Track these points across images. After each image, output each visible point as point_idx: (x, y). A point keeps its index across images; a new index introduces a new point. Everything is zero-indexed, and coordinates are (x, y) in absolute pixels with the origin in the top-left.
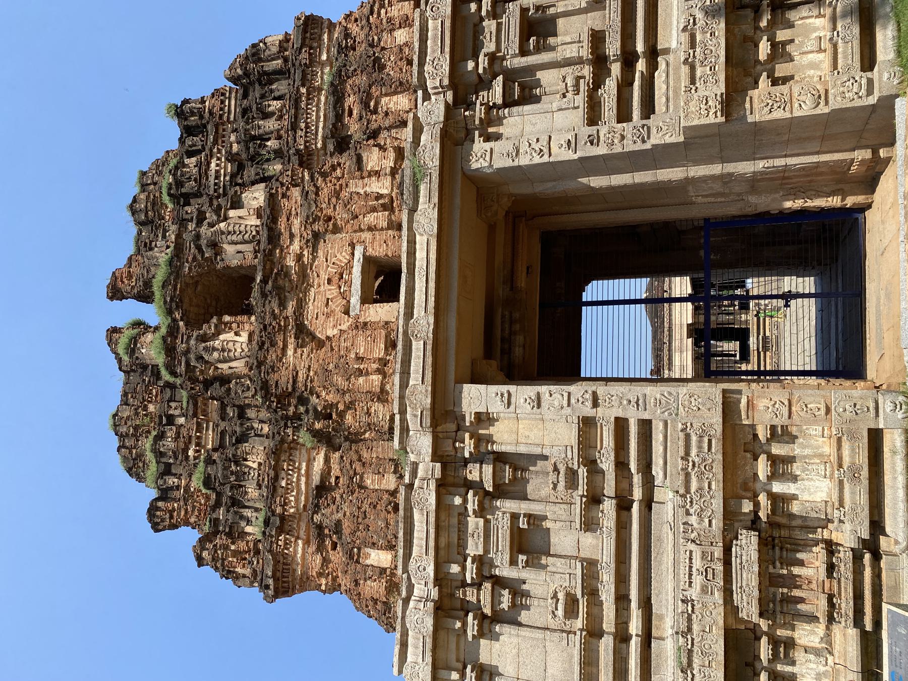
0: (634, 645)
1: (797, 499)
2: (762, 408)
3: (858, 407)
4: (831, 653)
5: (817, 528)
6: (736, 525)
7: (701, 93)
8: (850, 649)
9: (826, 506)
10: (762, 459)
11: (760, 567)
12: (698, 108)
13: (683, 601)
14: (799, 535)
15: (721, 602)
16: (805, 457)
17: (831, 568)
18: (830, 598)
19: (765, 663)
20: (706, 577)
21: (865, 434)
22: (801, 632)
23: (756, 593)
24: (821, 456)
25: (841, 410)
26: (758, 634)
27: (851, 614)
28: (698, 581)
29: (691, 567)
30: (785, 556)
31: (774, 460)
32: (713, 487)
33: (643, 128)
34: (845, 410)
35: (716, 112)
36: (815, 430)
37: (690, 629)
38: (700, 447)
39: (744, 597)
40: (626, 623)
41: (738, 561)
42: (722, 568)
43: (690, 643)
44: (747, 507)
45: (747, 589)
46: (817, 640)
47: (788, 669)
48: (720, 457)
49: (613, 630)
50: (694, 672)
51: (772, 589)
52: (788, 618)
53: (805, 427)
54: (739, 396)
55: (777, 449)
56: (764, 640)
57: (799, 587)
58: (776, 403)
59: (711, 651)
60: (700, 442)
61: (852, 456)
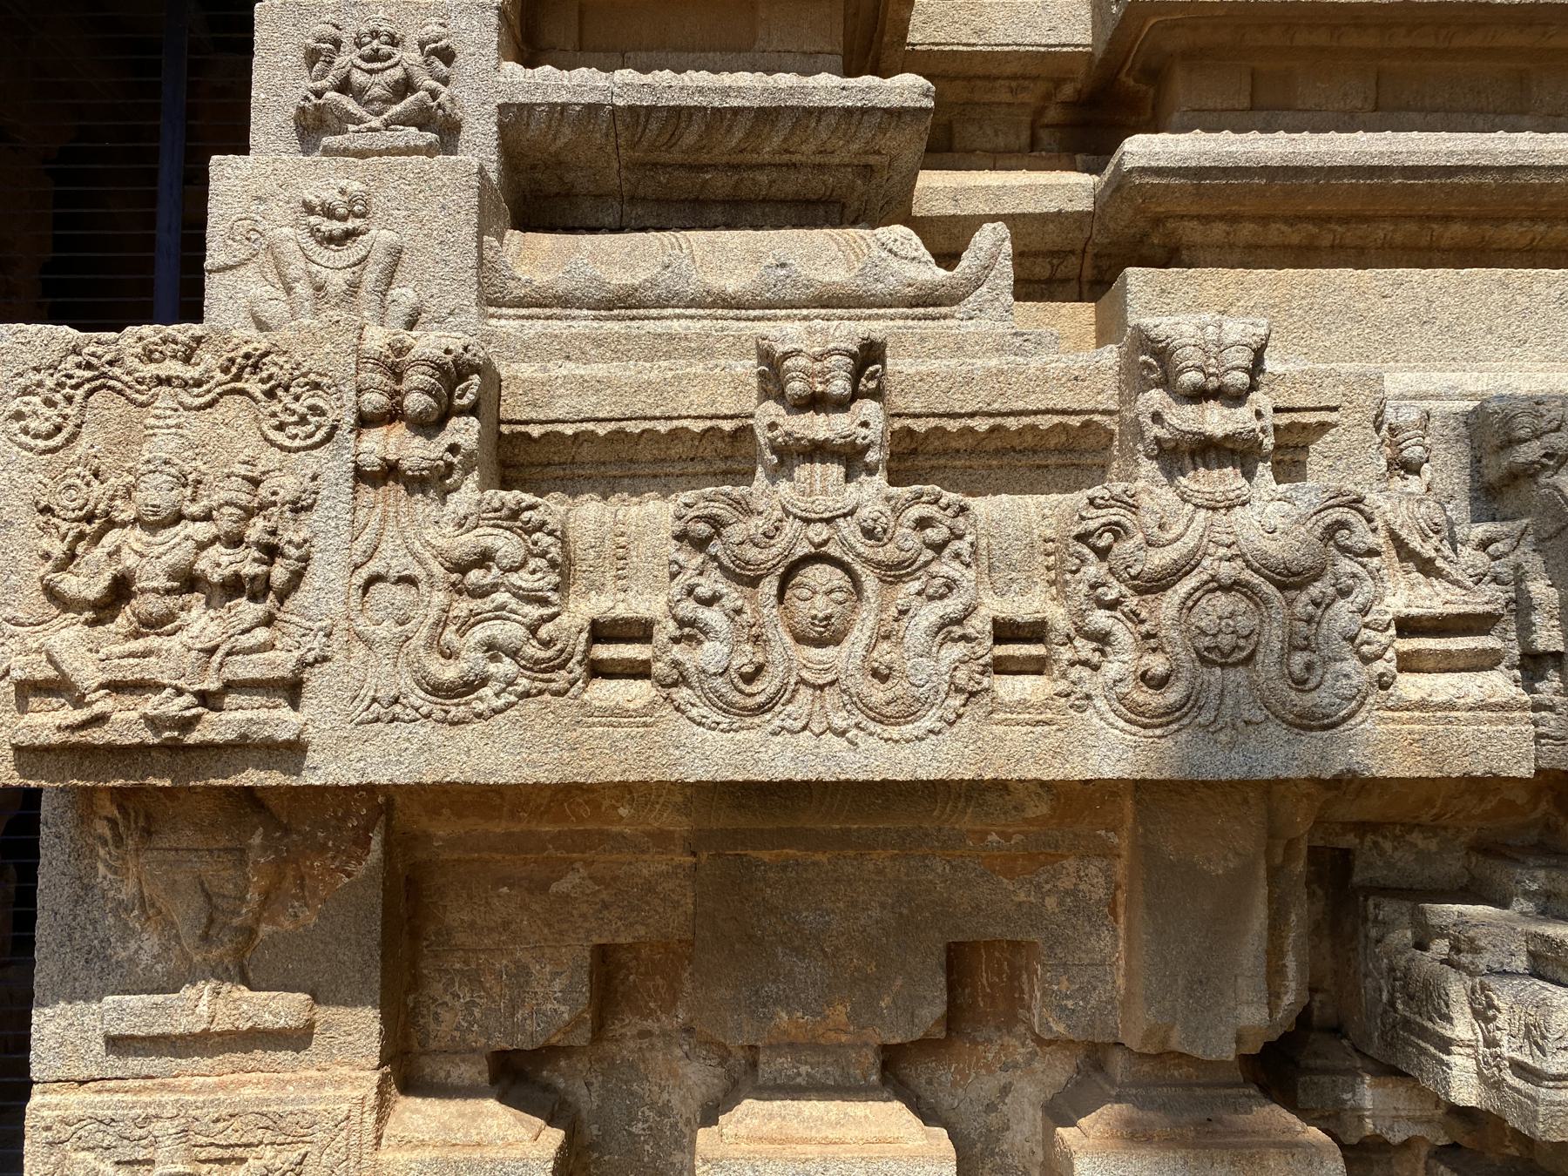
7: (334, 535)
12: (157, 494)
33: (422, 119)
35: (58, 687)
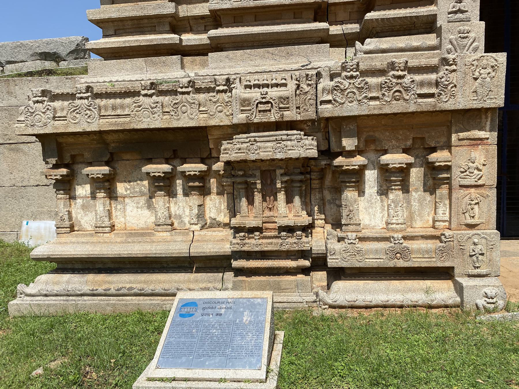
0: (171, 38)
1: (359, 195)
3: (480, 257)
4: (202, 228)
5: (324, 214)
6: (320, 135)
8: (210, 246)
9: (356, 224)
10: (410, 159)
11: (282, 160)
13: (228, 80)
14: (315, 197)
15: (235, 121)
16: (409, 202)
17: (290, 230)
18: (259, 229)
19: (180, 168)
20: (261, 103)
21: (447, 264)
22: (217, 201)
23: (252, 157)
24: (411, 217)
25: (476, 241)
26: (207, 161)
27: (245, 248)
28: (254, 95)
29: (267, 86)
30: (295, 185)
31: (404, 171)
32: (372, 103)
34: (475, 244)
37: (198, 91)
38: (422, 84)
39: (245, 145)
40: (191, 30)
41: (284, 137)
42: (273, 119)
43: (184, 90)
44: (349, 143)
45: (254, 147)
46: (213, 215)
47: (180, 190)
48: (412, 108)
49: (181, 14)
50: (154, 97)
51: (258, 173)
52: (230, 189)
54: (488, 128)
55: (416, 175)
56: (203, 167)
57: (264, 200)
58: (480, 170)
59: (180, 113)
60: (429, 84)
61: (419, 251)
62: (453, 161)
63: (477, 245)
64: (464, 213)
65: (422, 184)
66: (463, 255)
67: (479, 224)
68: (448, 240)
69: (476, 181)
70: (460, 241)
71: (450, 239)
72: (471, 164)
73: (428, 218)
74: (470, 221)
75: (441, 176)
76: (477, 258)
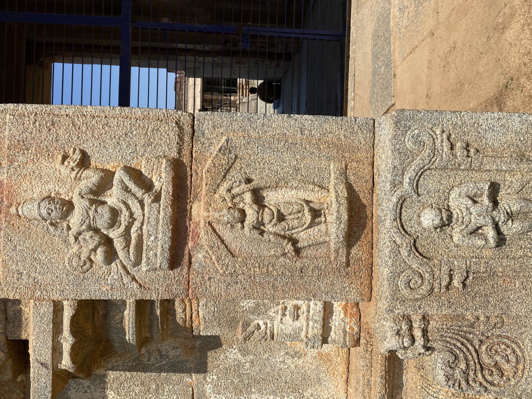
2: (30, 210)
3: (508, 201)
25: (429, 219)
34: (446, 222)
36: (290, 319)
53: (247, 304)
58: (106, 180)
62: (56, 297)
63: (450, 217)
64: (297, 251)
65: (175, 377)
66: (493, 274)
67: (350, 188)
68: (420, 341)
69: (157, 199)
70: (426, 288)
71: (418, 333)
72: (75, 219)
73: (309, 358)
74: (333, 229)
75: (130, 336)
76: (510, 216)
